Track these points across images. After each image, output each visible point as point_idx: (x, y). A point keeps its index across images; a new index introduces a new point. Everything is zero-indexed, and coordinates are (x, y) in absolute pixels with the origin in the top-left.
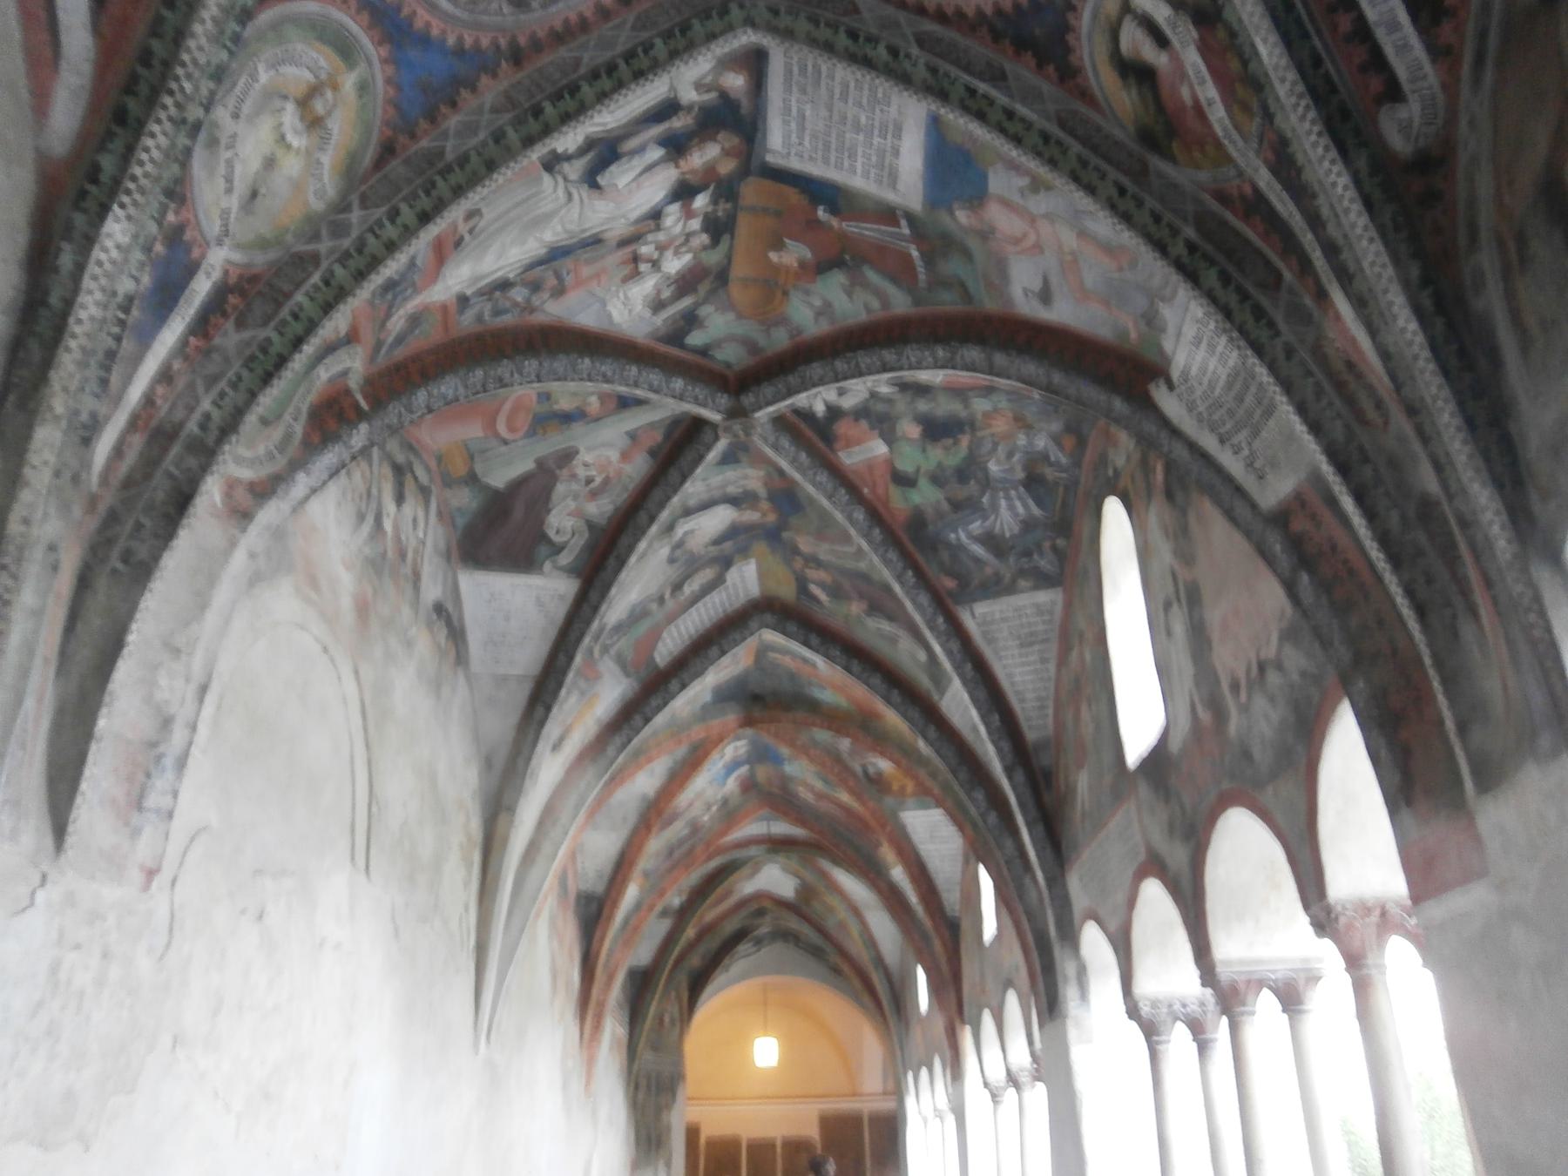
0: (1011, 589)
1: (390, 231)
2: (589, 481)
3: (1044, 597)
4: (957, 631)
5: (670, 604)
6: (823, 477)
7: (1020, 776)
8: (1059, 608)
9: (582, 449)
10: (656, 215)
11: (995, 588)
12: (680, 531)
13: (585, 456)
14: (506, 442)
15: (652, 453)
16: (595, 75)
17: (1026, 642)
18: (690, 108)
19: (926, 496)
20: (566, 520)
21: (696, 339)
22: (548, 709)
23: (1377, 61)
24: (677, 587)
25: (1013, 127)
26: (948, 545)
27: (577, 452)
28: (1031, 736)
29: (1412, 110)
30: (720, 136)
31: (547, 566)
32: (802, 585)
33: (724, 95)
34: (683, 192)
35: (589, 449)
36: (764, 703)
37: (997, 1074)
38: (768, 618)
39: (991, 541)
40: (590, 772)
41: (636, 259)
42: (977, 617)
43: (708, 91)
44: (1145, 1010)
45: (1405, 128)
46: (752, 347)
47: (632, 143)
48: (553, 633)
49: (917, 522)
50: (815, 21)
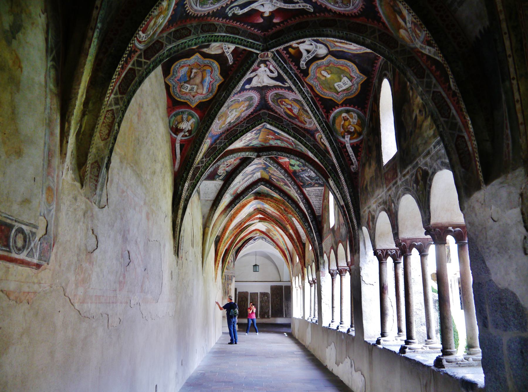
0: (313, 186)
1: (210, 162)
3: (320, 188)
4: (303, 193)
5: (242, 183)
6: (275, 165)
7: (314, 222)
8: (323, 191)
11: (310, 185)
16: (240, 133)
17: (317, 196)
19: (296, 168)
21: (251, 145)
22: (217, 207)
23: (350, 160)
24: (243, 179)
25: (306, 145)
26: (301, 177)
28: (317, 214)
29: (354, 166)
32: (270, 178)
36: (259, 196)
37: (311, 279)
38: (262, 183)
39: (309, 177)
40: (224, 216)
42: (306, 190)
44: (332, 271)
45: (354, 168)
46: (262, 145)
48: (218, 191)
49: (295, 172)
50: (276, 123)
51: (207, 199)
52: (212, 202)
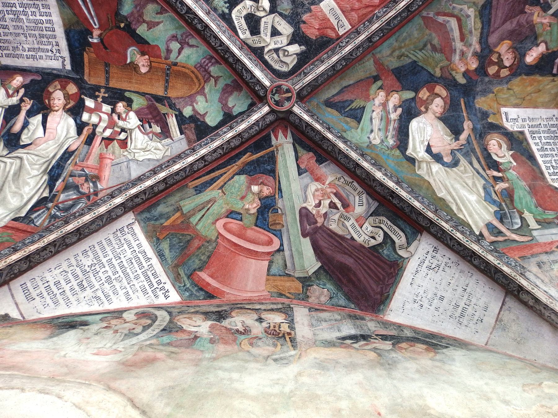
2: (333, 206)
9: (304, 205)
10: (80, 127)
12: (420, 153)
13: (311, 205)
14: (280, 250)
15: (320, 161)
18: (22, 100)
20: (362, 228)
27: (305, 208)
30: (51, 89)
31: (402, 253)
33: (24, 86)
34: (76, 110)
35: (306, 200)
41: (108, 140)
43: (18, 92)
47: (17, 128)
51: (490, 320)
52: (511, 303)
